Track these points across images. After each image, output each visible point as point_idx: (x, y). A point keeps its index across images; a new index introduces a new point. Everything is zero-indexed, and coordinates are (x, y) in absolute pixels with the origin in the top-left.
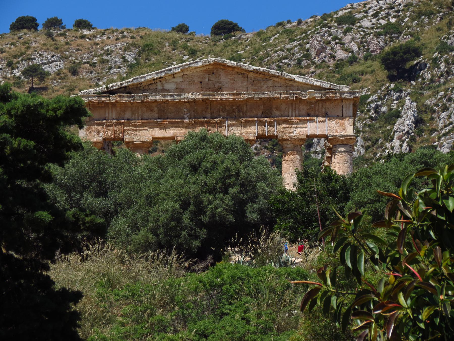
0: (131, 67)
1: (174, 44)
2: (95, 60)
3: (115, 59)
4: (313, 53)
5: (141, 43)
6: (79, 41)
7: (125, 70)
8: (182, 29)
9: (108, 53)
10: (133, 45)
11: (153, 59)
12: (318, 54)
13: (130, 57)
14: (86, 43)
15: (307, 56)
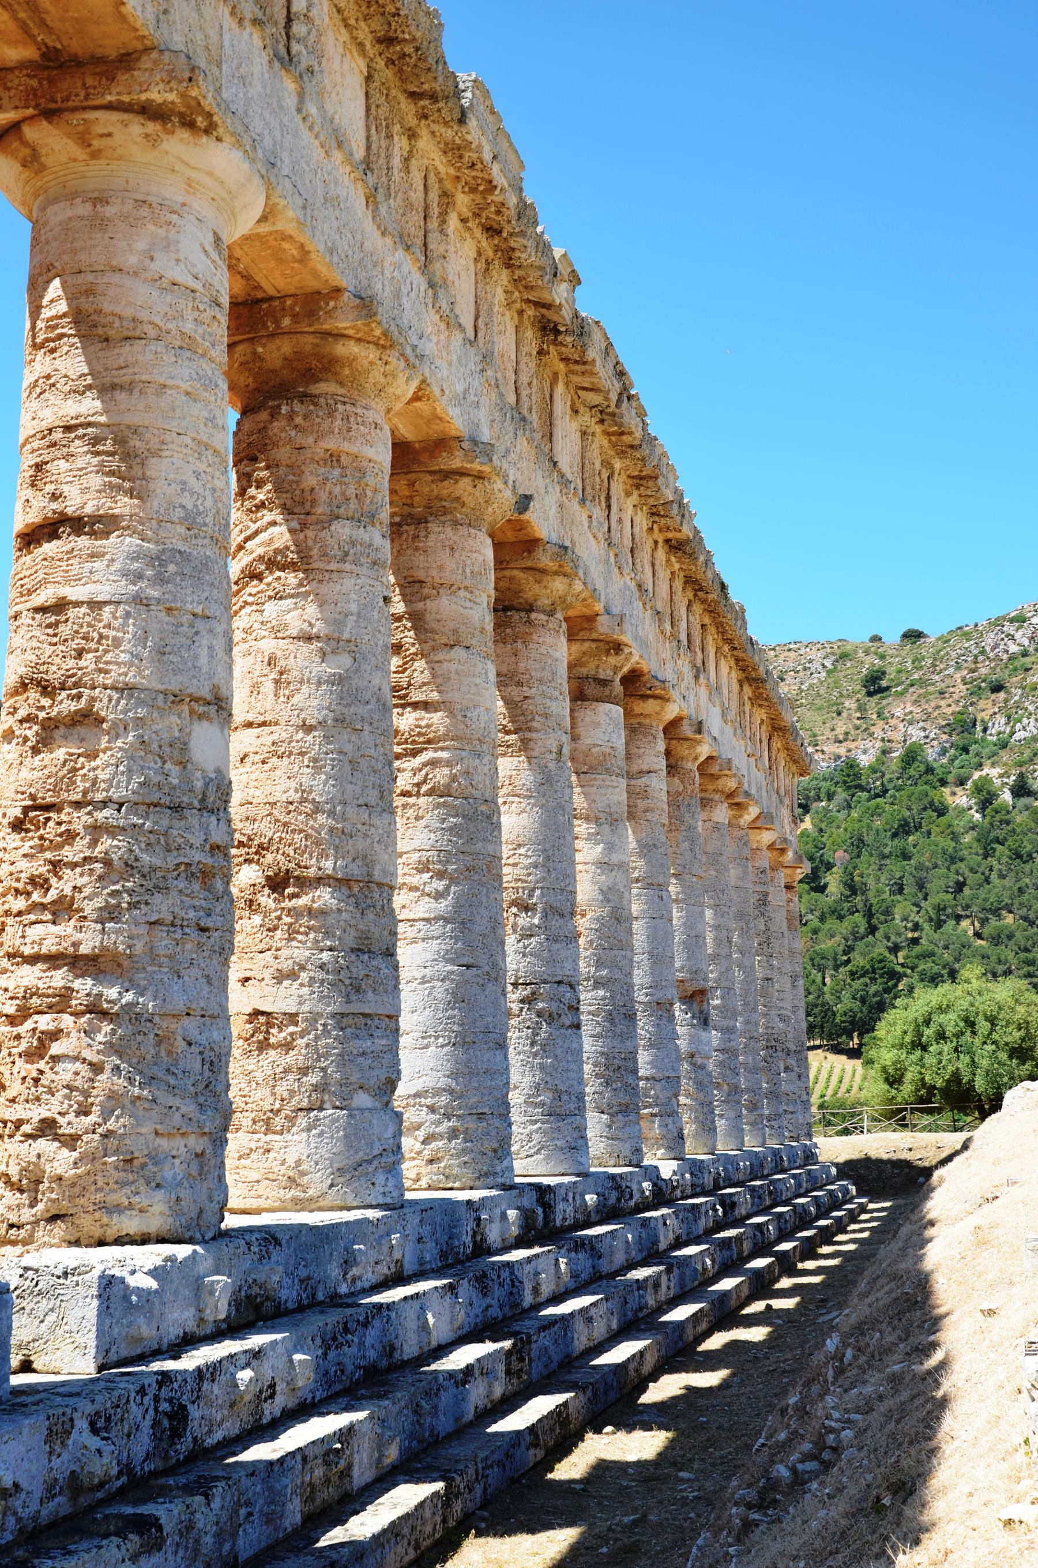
0: (829, 672)
1: (867, 653)
2: (800, 668)
3: (817, 665)
4: (988, 649)
5: (838, 652)
6: (787, 654)
7: (824, 674)
8: (876, 639)
9: (810, 661)
10: (833, 654)
11: (849, 664)
12: (992, 650)
13: (828, 664)
14: (792, 654)
15: (983, 652)
